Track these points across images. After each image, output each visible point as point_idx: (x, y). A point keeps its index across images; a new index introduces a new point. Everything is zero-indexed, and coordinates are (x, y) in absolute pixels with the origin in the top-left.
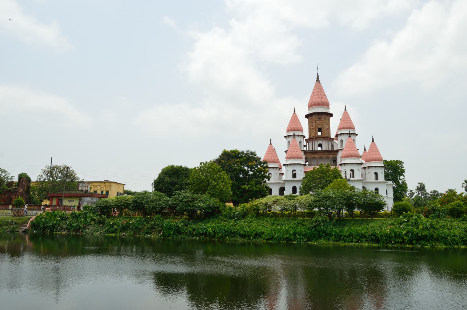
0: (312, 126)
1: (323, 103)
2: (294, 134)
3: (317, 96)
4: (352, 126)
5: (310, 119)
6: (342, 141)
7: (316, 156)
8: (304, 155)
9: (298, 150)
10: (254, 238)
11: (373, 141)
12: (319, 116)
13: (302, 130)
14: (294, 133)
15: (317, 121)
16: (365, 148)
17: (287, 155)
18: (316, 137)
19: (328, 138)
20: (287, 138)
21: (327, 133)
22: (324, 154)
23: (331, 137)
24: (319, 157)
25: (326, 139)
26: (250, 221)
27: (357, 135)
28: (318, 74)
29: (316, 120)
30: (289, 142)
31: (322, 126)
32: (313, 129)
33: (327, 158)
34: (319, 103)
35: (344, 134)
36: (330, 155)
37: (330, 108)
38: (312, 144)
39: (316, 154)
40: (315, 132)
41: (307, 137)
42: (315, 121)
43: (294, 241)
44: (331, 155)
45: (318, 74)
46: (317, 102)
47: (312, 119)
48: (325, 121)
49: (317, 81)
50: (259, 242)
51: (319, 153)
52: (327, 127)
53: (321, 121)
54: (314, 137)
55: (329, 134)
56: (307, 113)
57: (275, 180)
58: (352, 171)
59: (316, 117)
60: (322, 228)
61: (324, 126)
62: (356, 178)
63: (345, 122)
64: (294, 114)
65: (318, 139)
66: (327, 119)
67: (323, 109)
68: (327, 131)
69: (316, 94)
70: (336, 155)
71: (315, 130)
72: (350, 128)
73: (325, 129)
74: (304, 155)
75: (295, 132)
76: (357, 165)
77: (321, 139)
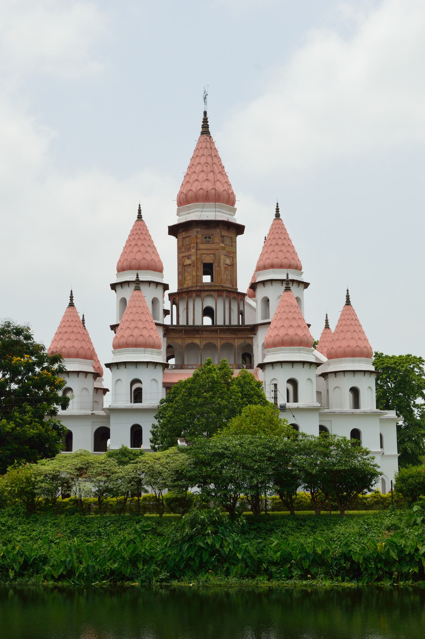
0: (189, 257)
1: (219, 196)
2: (137, 277)
3: (202, 176)
4: (293, 262)
5: (183, 238)
6: (266, 301)
9: (147, 325)
10: (19, 574)
11: (348, 303)
12: (207, 232)
13: (159, 269)
14: (137, 275)
15: (202, 243)
16: (327, 321)
17: (116, 337)
18: (198, 288)
19: (230, 292)
20: (119, 288)
21: (229, 277)
22: (219, 336)
23: (239, 291)
24: (204, 344)
25: (225, 294)
26: (8, 528)
27: (306, 285)
28: (205, 113)
29: (199, 241)
30: (123, 301)
31: (215, 258)
32: (190, 265)
33: (227, 347)
35: (272, 281)
36: (234, 339)
37: (236, 209)
38: (187, 308)
39: (197, 336)
40: (194, 273)
41: (174, 288)
42: (197, 245)
43: (132, 580)
44: (236, 340)
45: (205, 113)
47: (187, 237)
48: (223, 245)
49: (202, 133)
50: (33, 588)
51: (204, 332)
52: (228, 261)
54: (191, 287)
55: (234, 281)
56: (175, 221)
57: (81, 409)
58: (293, 382)
59: (197, 232)
60: (209, 541)
61: (220, 259)
62: (301, 404)
63: (277, 249)
64: (140, 223)
65: (204, 294)
66: (227, 241)
67: (219, 212)
68: (227, 272)
69: (198, 168)
70: (252, 338)
72: (290, 267)
73: (223, 268)
74: (165, 339)
75: (139, 272)
76: (307, 366)
77: (211, 296)
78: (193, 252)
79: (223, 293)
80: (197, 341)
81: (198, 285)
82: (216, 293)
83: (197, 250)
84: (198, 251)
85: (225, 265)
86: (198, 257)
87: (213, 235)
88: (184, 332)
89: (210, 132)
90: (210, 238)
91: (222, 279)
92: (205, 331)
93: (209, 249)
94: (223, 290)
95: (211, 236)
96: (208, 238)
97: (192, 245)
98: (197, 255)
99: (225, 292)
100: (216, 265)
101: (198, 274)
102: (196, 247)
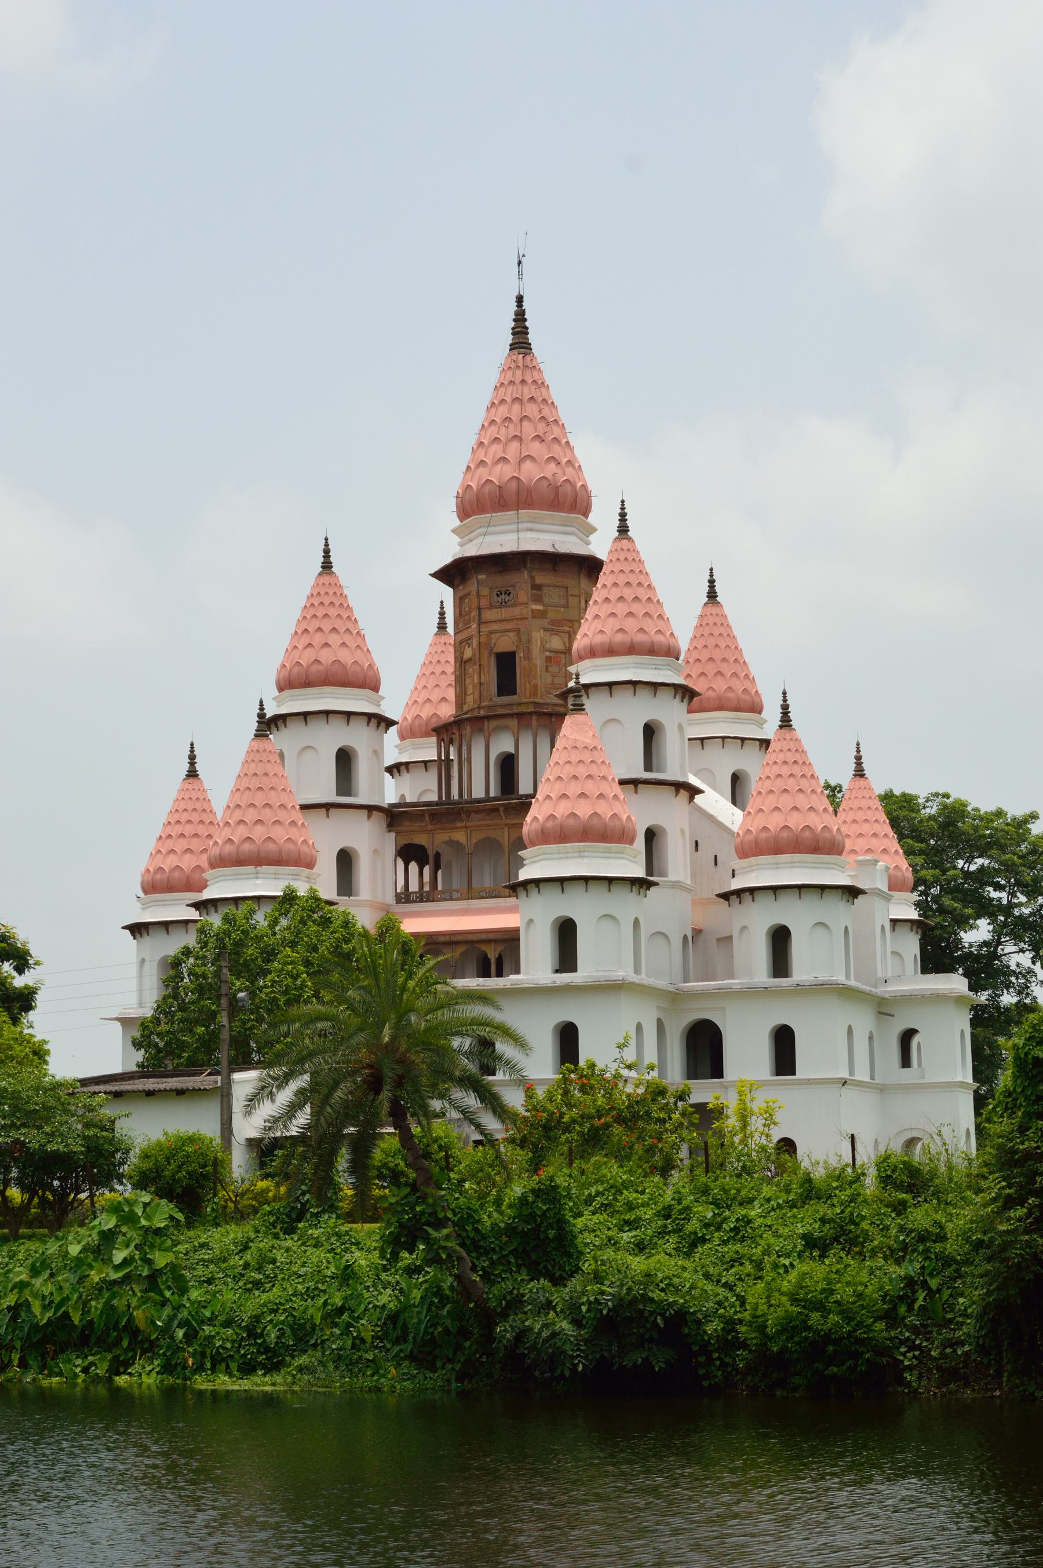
7: (460, 836)
8: (393, 835)
12: (500, 581)
15: (491, 607)
16: (858, 758)
18: (482, 712)
24: (474, 841)
28: (520, 300)
29: (484, 602)
31: (520, 640)
32: (470, 659)
34: (501, 495)
39: (459, 824)
45: (520, 300)
46: (487, 489)
48: (540, 607)
49: (513, 347)
51: (473, 815)
52: (556, 643)
53: (515, 605)
61: (529, 641)
62: (581, 976)
63: (621, 609)
64: (326, 579)
71: (477, 667)
77: (506, 728)
79: (531, 719)
80: (460, 836)
81: (483, 704)
82: (516, 721)
85: (548, 654)
86: (483, 639)
88: (427, 818)
89: (530, 344)
90: (509, 595)
91: (535, 687)
92: (477, 811)
93: (506, 620)
94: (531, 713)
96: (505, 593)
98: (480, 636)
99: (534, 717)
100: (522, 655)
101: (482, 681)
102: (477, 618)
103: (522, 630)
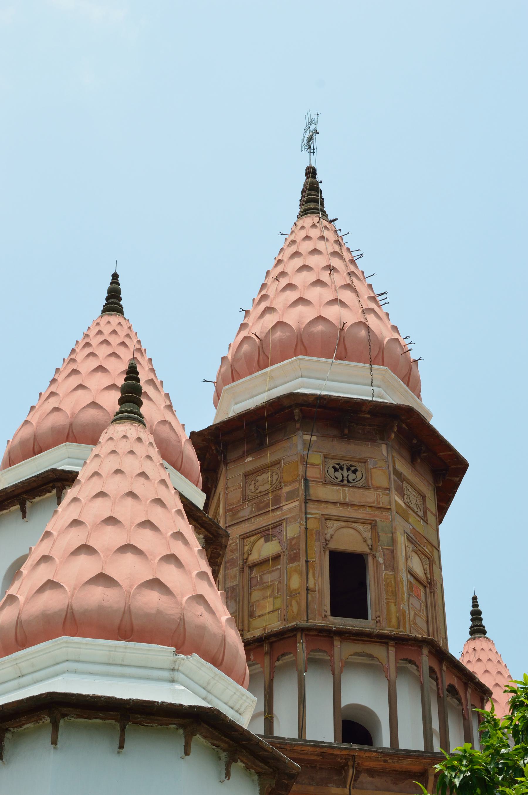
5: (246, 475)
15: (326, 483)
28: (311, 172)
29: (312, 473)
40: (295, 582)
42: (307, 487)
45: (311, 172)
47: (263, 470)
53: (366, 487)
59: (309, 446)
78: (290, 510)
82: (392, 651)
83: (306, 503)
84: (310, 505)
87: (364, 461)
90: (355, 472)
93: (352, 505)
95: (358, 466)
96: (348, 469)
97: (285, 490)
98: (307, 519)
100: (381, 560)
101: (311, 584)
102: (301, 492)
103: (379, 524)
